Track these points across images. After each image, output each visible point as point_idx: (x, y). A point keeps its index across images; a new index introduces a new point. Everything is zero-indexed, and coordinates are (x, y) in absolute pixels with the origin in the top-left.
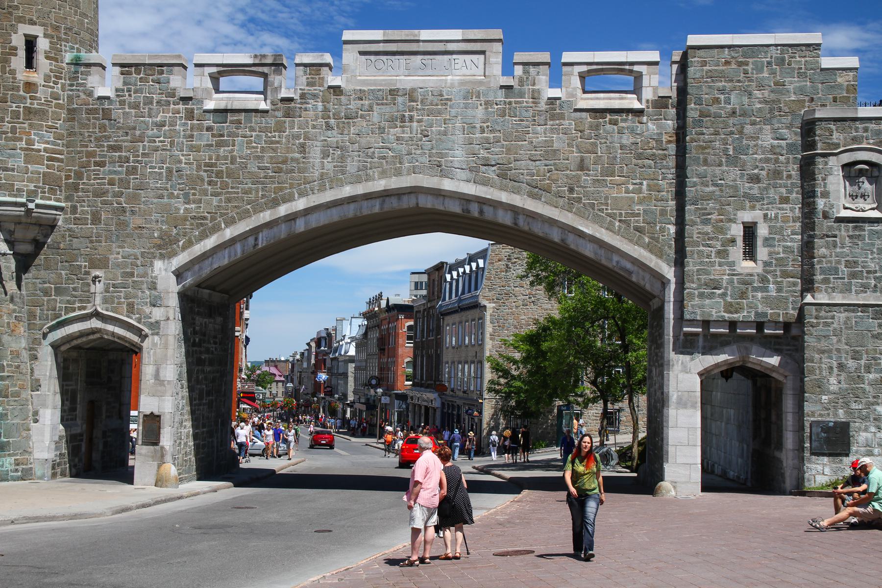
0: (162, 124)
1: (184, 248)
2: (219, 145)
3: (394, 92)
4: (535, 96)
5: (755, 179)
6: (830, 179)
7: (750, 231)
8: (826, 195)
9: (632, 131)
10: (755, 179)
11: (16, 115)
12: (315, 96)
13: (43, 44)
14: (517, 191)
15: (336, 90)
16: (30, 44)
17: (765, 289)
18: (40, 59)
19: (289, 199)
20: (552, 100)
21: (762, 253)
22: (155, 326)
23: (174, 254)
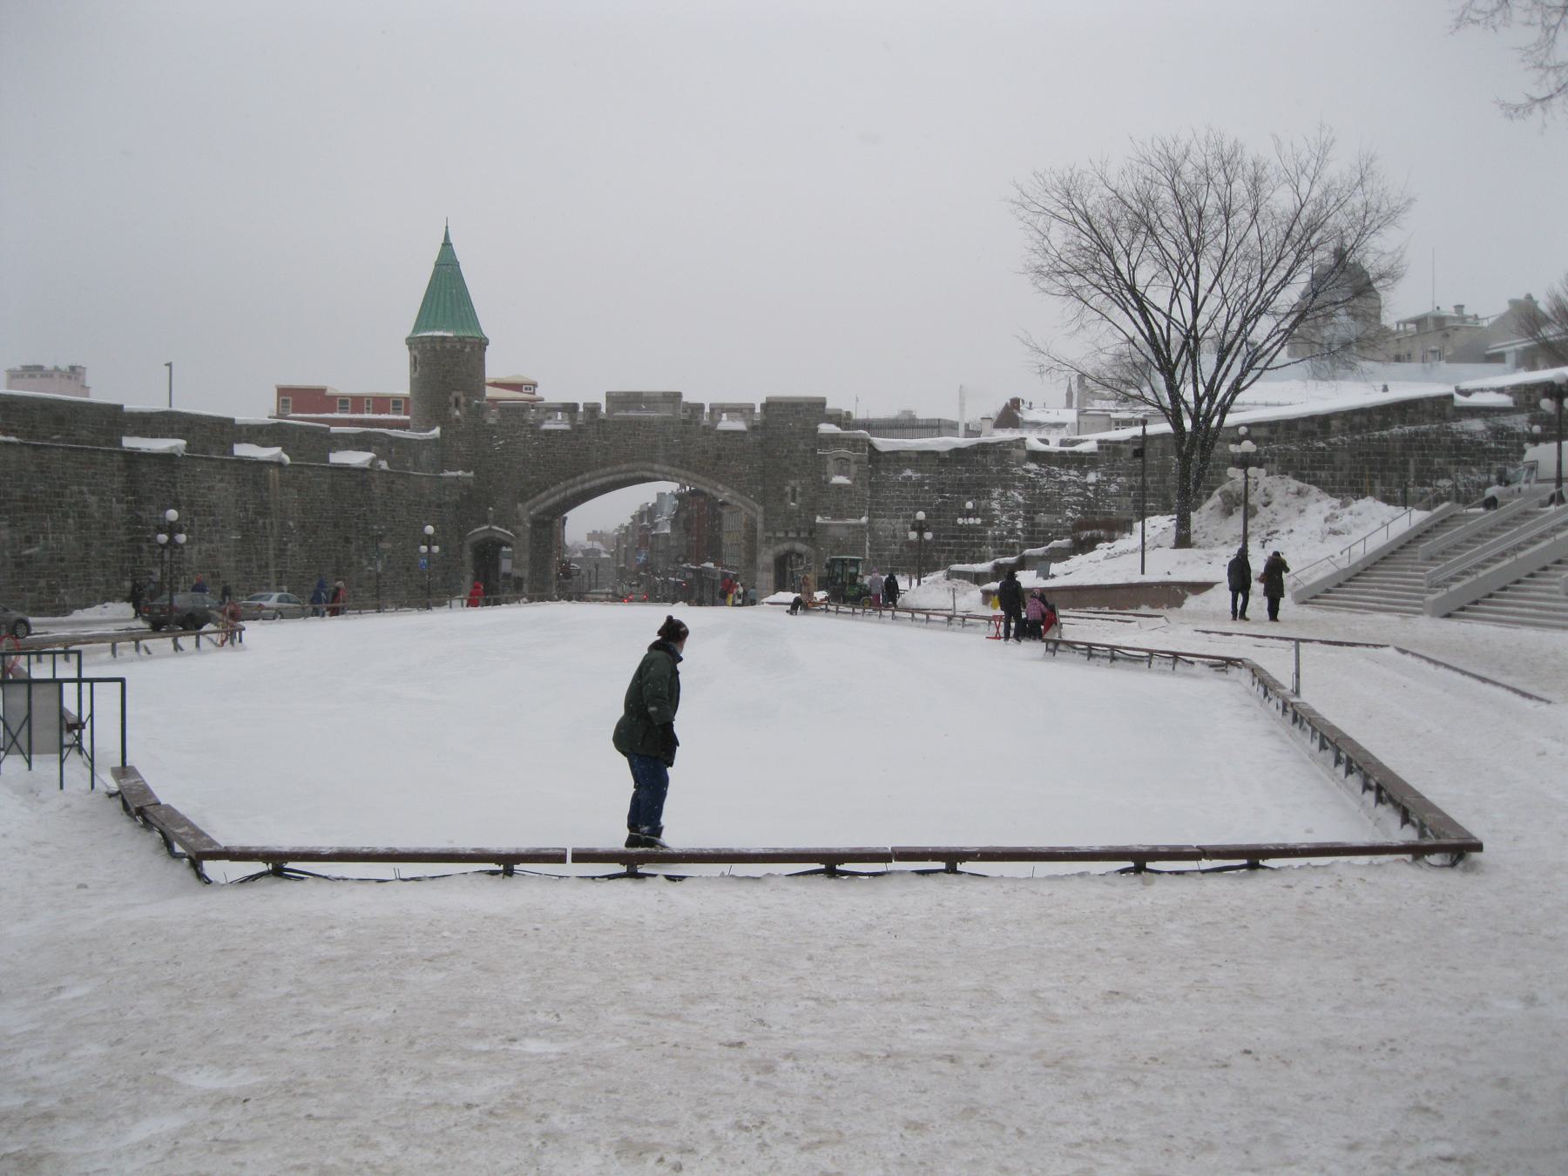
0: (519, 437)
1: (532, 497)
2: (548, 447)
3: (630, 422)
4: (698, 423)
5: (796, 465)
6: (828, 466)
7: (794, 490)
8: (826, 473)
9: (742, 441)
10: (796, 465)
11: (451, 435)
12: (592, 423)
13: (463, 400)
14: (688, 469)
15: (604, 421)
16: (457, 401)
17: (800, 516)
18: (462, 406)
19: (581, 473)
20: (704, 427)
21: (799, 499)
22: (517, 535)
23: (527, 500)
